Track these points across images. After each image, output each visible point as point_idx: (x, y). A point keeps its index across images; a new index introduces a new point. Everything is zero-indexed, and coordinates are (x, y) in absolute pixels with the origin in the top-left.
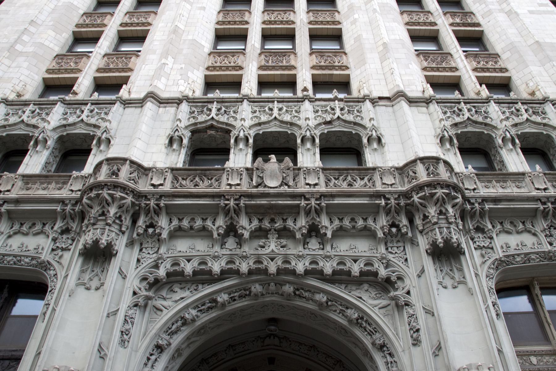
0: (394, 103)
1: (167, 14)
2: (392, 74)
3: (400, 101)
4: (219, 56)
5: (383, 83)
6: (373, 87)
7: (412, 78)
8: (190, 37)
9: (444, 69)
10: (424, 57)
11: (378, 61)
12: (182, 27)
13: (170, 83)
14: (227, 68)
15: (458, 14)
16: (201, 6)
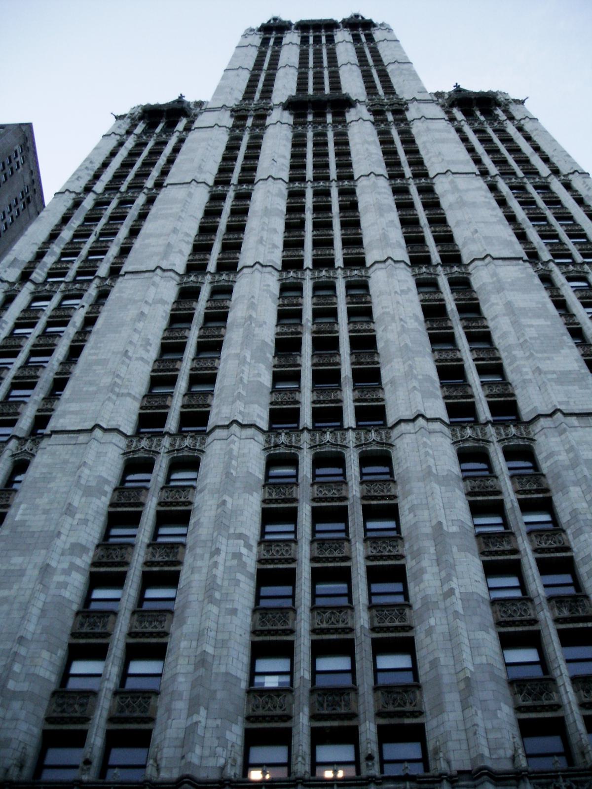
0: (477, 782)
1: (189, 622)
2: (475, 734)
3: (484, 782)
4: (261, 696)
5: (464, 747)
6: (451, 753)
7: (499, 735)
8: (223, 669)
9: (543, 708)
10: (518, 686)
11: (458, 706)
12: (210, 650)
13: (207, 752)
14: (272, 719)
15: (566, 599)
16: (231, 607)
